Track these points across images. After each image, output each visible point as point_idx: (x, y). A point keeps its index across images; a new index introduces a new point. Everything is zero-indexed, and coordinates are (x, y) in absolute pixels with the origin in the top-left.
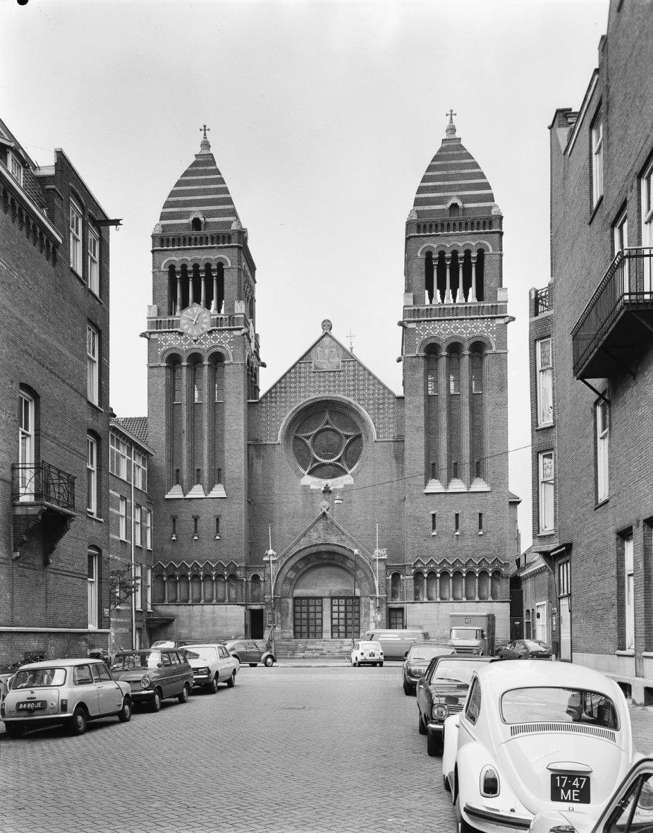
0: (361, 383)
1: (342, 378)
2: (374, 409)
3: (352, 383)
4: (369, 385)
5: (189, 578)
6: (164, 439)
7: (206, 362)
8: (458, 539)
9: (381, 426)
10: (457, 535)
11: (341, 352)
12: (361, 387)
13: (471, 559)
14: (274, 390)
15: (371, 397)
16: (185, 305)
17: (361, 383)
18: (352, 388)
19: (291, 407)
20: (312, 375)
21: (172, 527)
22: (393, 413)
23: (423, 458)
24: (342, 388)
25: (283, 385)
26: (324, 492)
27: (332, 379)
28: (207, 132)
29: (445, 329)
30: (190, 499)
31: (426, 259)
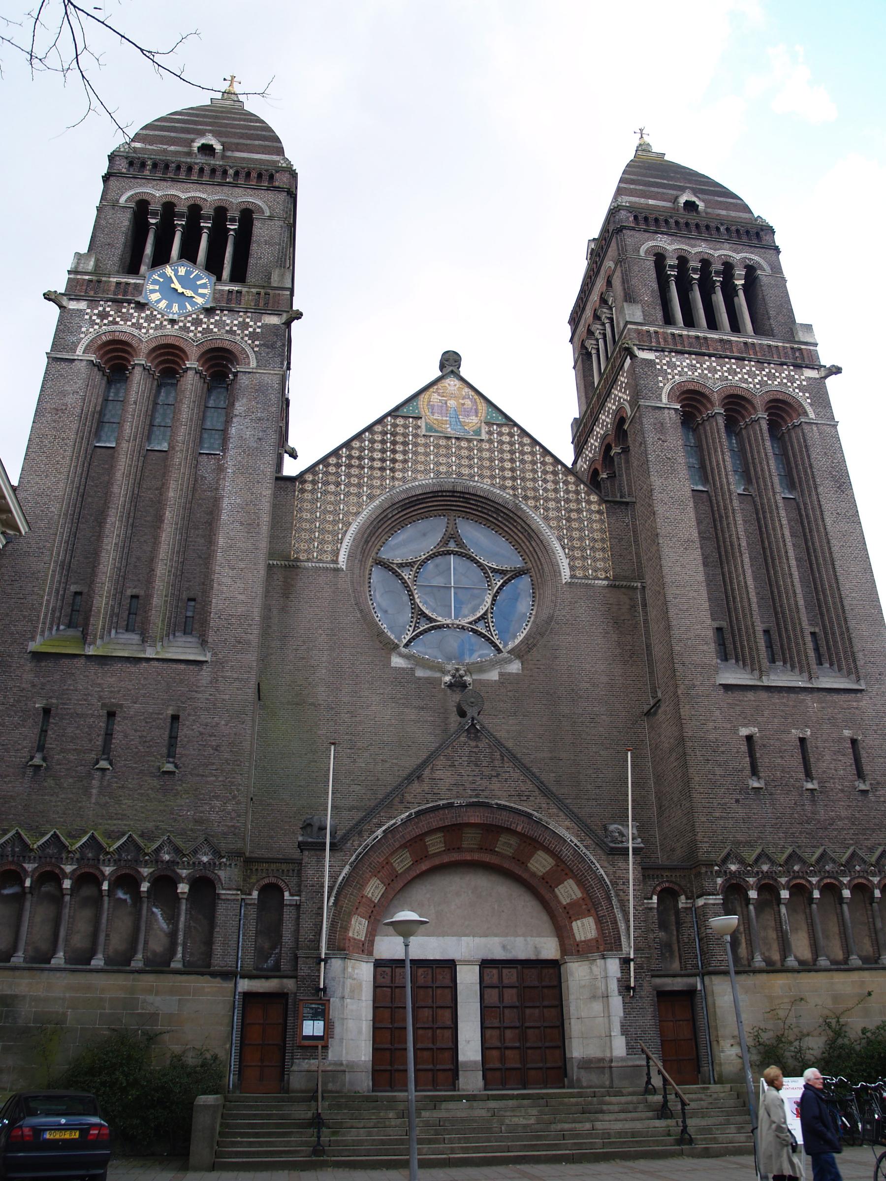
2: (559, 519)
4: (545, 472)
5: (67, 884)
6: (55, 508)
7: (191, 363)
8: (813, 801)
9: (578, 554)
10: (812, 790)
11: (482, 406)
12: (529, 475)
13: (854, 855)
15: (551, 495)
16: (161, 258)
18: (508, 474)
19: (371, 497)
20: (421, 441)
21: (37, 730)
22: (602, 531)
23: (706, 605)
24: (487, 473)
26: (450, 686)
27: (464, 453)
30: (103, 660)
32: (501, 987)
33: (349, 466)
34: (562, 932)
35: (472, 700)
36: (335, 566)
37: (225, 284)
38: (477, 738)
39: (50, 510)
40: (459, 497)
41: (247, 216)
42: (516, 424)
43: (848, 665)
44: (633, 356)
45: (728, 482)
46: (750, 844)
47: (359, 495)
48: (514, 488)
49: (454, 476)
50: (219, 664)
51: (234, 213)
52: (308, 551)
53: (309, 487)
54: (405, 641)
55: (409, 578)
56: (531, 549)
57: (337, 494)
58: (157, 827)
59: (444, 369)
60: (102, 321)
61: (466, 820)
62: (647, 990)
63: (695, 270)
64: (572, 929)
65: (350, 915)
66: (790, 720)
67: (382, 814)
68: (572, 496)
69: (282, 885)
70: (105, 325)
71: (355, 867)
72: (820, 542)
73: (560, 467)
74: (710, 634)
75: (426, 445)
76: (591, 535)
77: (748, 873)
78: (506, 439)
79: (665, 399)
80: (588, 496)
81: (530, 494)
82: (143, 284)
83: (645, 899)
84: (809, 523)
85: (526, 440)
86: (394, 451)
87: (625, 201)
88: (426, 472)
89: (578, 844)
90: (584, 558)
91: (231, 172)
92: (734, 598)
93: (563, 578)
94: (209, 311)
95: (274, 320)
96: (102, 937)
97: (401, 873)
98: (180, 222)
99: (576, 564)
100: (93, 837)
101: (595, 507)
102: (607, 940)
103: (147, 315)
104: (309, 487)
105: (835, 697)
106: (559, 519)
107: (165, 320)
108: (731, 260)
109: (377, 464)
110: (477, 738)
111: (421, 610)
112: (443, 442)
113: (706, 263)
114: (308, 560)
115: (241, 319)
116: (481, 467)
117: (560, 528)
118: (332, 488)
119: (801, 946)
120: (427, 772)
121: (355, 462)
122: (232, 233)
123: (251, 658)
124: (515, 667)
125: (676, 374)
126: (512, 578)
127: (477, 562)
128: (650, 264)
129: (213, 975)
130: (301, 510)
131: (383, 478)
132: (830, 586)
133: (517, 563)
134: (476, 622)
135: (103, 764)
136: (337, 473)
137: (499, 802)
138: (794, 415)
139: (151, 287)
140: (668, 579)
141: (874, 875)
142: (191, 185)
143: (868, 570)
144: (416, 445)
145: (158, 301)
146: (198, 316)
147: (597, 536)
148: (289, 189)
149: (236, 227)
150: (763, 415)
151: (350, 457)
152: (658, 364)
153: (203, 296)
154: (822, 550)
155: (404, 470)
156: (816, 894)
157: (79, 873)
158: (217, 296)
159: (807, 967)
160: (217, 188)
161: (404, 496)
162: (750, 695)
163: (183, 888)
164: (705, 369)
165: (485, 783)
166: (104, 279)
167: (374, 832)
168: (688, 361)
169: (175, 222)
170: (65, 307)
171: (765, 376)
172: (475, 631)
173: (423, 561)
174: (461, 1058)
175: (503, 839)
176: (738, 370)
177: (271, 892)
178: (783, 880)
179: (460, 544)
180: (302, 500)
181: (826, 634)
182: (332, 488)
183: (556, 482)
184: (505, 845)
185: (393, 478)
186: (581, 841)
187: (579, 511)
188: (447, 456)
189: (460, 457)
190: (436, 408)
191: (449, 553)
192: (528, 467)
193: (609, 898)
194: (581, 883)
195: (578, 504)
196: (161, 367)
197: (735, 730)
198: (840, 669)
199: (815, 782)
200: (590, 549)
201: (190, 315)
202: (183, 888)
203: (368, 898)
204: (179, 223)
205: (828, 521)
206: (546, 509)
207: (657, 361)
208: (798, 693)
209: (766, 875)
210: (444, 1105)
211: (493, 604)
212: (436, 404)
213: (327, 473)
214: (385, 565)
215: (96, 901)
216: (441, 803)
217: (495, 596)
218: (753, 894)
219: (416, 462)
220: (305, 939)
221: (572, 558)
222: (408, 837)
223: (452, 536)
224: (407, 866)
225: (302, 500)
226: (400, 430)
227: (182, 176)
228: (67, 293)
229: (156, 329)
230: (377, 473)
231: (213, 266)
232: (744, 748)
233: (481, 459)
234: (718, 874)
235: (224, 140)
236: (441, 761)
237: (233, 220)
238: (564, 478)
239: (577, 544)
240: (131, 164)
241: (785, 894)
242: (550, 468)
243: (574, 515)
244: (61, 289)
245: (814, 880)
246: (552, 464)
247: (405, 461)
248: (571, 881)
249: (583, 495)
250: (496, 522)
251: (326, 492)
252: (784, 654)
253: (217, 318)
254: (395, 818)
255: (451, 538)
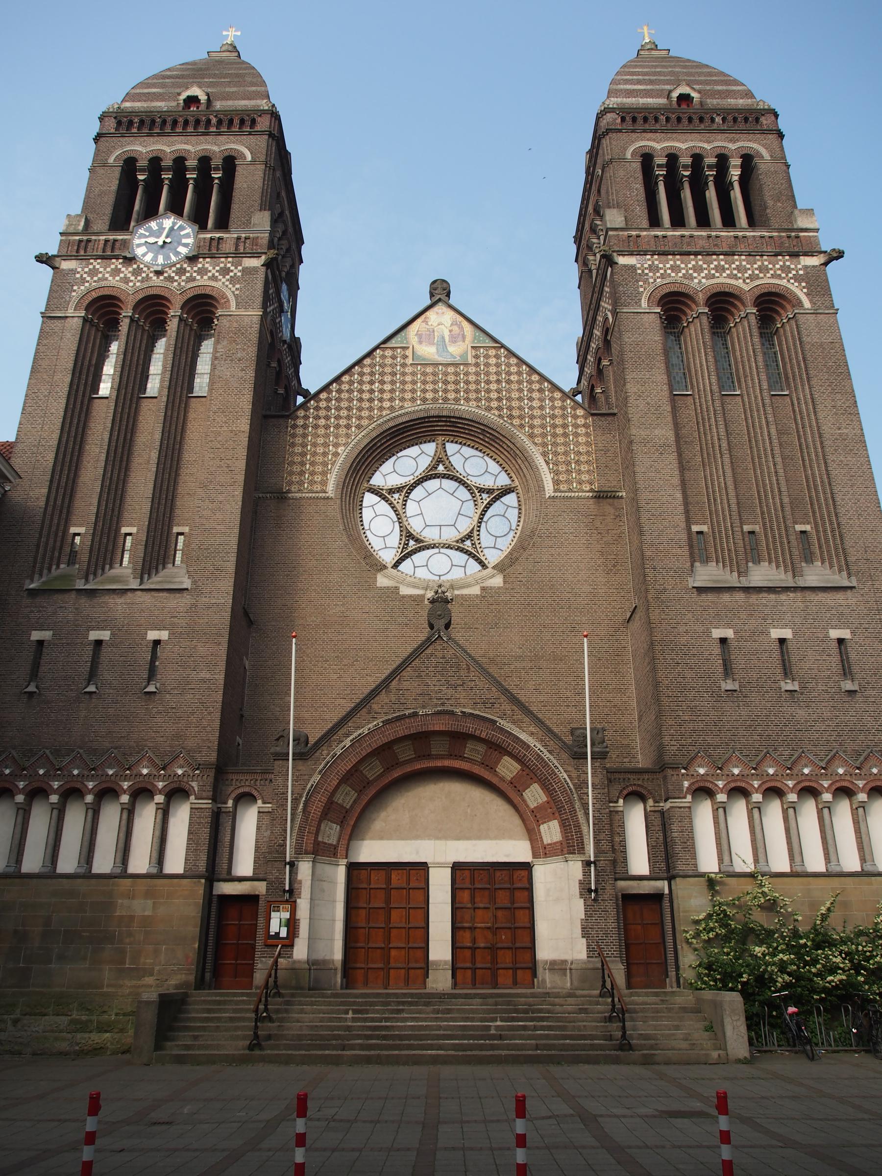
2: (544, 435)
4: (531, 391)
16: (150, 212)
22: (587, 444)
34: (533, 836)
35: (439, 613)
36: (324, 495)
39: (45, 459)
40: (446, 421)
42: (503, 346)
43: (839, 562)
45: (710, 382)
48: (499, 409)
49: (440, 401)
51: (217, 162)
52: (301, 483)
55: (398, 502)
56: (517, 467)
59: (433, 298)
60: (92, 278)
61: (431, 728)
62: (608, 893)
63: (685, 167)
64: (539, 830)
67: (350, 725)
68: (557, 412)
69: (255, 793)
70: (95, 282)
72: (812, 437)
73: (546, 384)
76: (576, 449)
78: (493, 361)
79: (644, 303)
80: (575, 410)
82: (130, 240)
83: (610, 802)
84: (802, 418)
86: (382, 382)
87: (612, 103)
89: (542, 749)
91: (214, 121)
92: (715, 500)
93: (547, 493)
94: (192, 259)
97: (373, 780)
98: (167, 176)
99: (561, 478)
101: (581, 421)
102: (570, 843)
103: (134, 269)
107: (151, 272)
108: (726, 152)
111: (409, 532)
113: (697, 159)
114: (300, 491)
117: (545, 445)
120: (394, 683)
124: (498, 581)
125: (658, 278)
128: (637, 166)
132: (822, 482)
133: (503, 480)
137: (464, 710)
138: (788, 306)
140: (641, 485)
142: (176, 138)
145: (144, 255)
146: (182, 265)
147: (583, 449)
148: (270, 132)
149: (220, 175)
152: (639, 269)
153: (186, 245)
154: (814, 445)
157: (30, 788)
158: (198, 245)
160: (201, 138)
164: (690, 269)
165: (450, 692)
167: (342, 741)
169: (163, 177)
170: (58, 268)
171: (756, 269)
173: (411, 486)
174: (432, 957)
175: (470, 745)
176: (727, 266)
179: (449, 467)
181: (817, 531)
183: (541, 400)
186: (545, 746)
190: (424, 336)
192: (515, 386)
194: (546, 787)
195: (564, 419)
197: (708, 633)
198: (831, 567)
199: (796, 683)
200: (575, 463)
201: (174, 265)
203: (339, 804)
204: (166, 176)
206: (532, 427)
208: (778, 593)
212: (424, 333)
216: (407, 712)
220: (275, 843)
222: (375, 746)
224: (378, 773)
227: (168, 129)
228: (60, 254)
229: (142, 281)
237: (217, 169)
238: (551, 395)
239: (561, 458)
240: (119, 123)
242: (536, 386)
246: (538, 382)
248: (536, 786)
249: (569, 410)
250: (484, 443)
252: (769, 554)
254: (362, 727)
255: (439, 462)
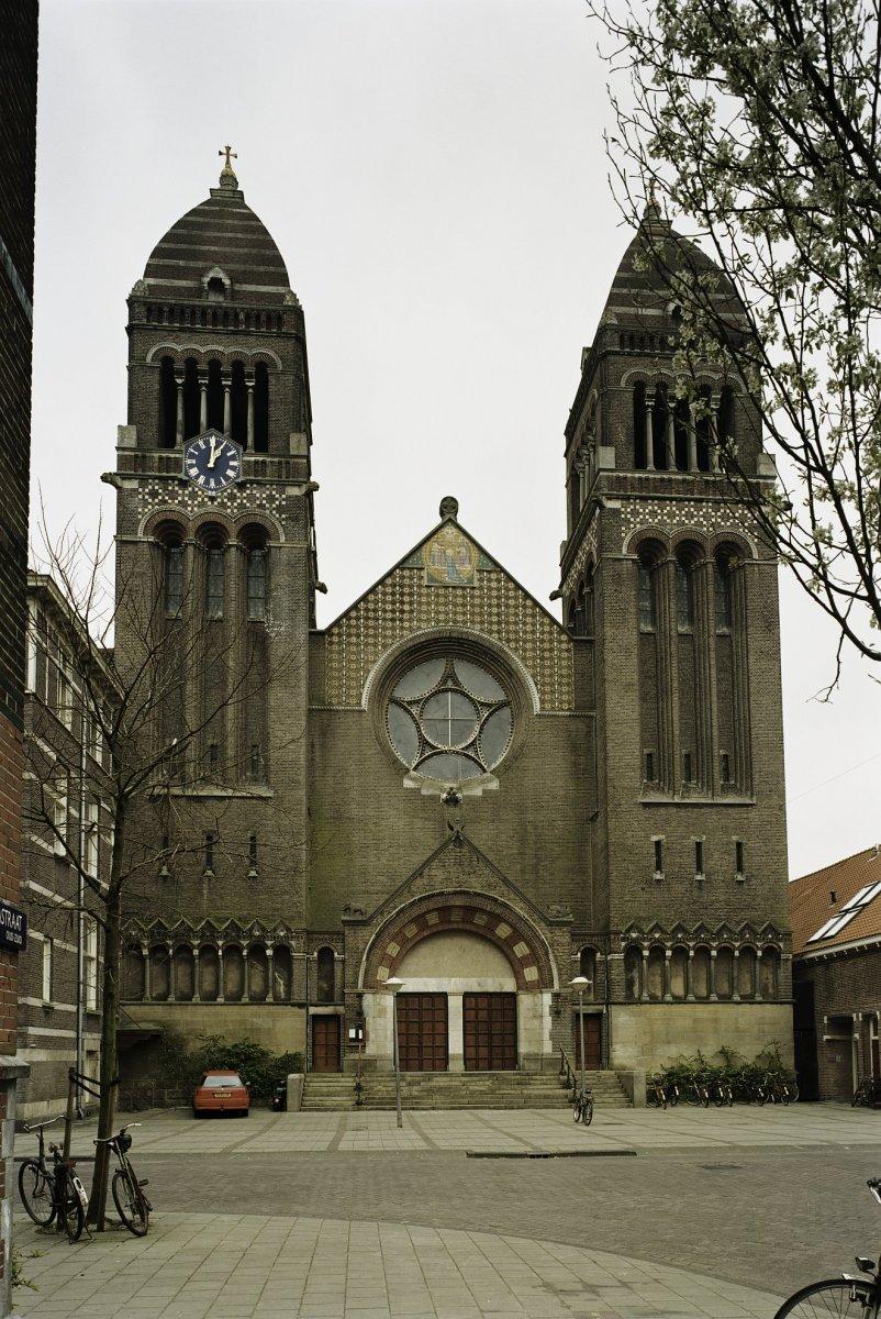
0: (512, 611)
1: (477, 601)
3: (495, 610)
4: (525, 615)
8: (700, 888)
10: (700, 881)
11: (475, 553)
12: (512, 619)
13: (724, 926)
14: (353, 614)
15: (529, 637)
17: (512, 611)
18: (495, 619)
19: (385, 646)
20: (424, 591)
22: (569, 667)
24: (477, 619)
25: (371, 606)
27: (460, 601)
28: (232, 158)
29: (671, 515)
31: (635, 392)
32: (477, 1010)
33: (367, 618)
34: (518, 975)
37: (251, 455)
38: (461, 846)
41: (262, 368)
42: (503, 570)
44: (602, 507)
46: (649, 919)
47: (375, 645)
48: (499, 632)
50: (280, 799)
52: (339, 696)
53: (335, 639)
54: (414, 765)
57: (358, 645)
58: (249, 914)
65: (377, 967)
66: (691, 829)
69: (333, 948)
71: (378, 936)
74: (637, 762)
75: (428, 595)
77: (644, 940)
78: (494, 585)
81: (512, 636)
85: (511, 585)
86: (402, 603)
88: (428, 621)
90: (552, 692)
95: (295, 491)
96: (222, 985)
100: (208, 921)
104: (335, 639)
105: (730, 810)
106: (534, 658)
109: (389, 615)
110: (461, 846)
112: (441, 591)
114: (339, 703)
115: (268, 492)
116: (472, 614)
117: (534, 667)
118: (354, 639)
119: (677, 987)
120: (426, 870)
121: (371, 614)
122: (250, 390)
123: (302, 793)
124: (494, 785)
126: (496, 710)
127: (469, 697)
129: (292, 1005)
130: (331, 661)
131: (393, 628)
133: (500, 696)
134: (467, 748)
135: (209, 873)
136: (357, 625)
139: (189, 461)
140: (609, 718)
141: (737, 941)
143: (779, 702)
144: (420, 595)
150: (711, 559)
151: (367, 610)
155: (410, 620)
156: (692, 953)
159: (678, 1000)
161: (411, 644)
162: (662, 811)
163: (269, 952)
166: (148, 454)
168: (650, 508)
172: (467, 756)
177: (326, 955)
178: (669, 944)
179: (456, 682)
180: (331, 652)
182: (354, 639)
183: (534, 625)
184: (480, 920)
185: (402, 628)
187: (551, 650)
188: (446, 604)
189: (455, 605)
191: (447, 690)
193: (547, 954)
196: (209, 541)
197: (647, 837)
202: (269, 952)
205: (751, 661)
207: (623, 509)
209: (657, 940)
210: (435, 1079)
211: (480, 732)
213: (349, 626)
214: (399, 704)
215: (215, 961)
217: (483, 726)
218: (646, 953)
219: (420, 612)
221: (542, 693)
223: (450, 675)
225: (331, 652)
226: (407, 581)
230: (389, 624)
231: (238, 436)
232: (653, 851)
233: (473, 606)
234: (623, 939)
235: (231, 266)
236: (435, 863)
239: (547, 680)
241: (669, 953)
243: (547, 654)
244: (113, 469)
245: (691, 944)
246: (531, 607)
247: (411, 612)
251: (349, 644)
253: (248, 492)
